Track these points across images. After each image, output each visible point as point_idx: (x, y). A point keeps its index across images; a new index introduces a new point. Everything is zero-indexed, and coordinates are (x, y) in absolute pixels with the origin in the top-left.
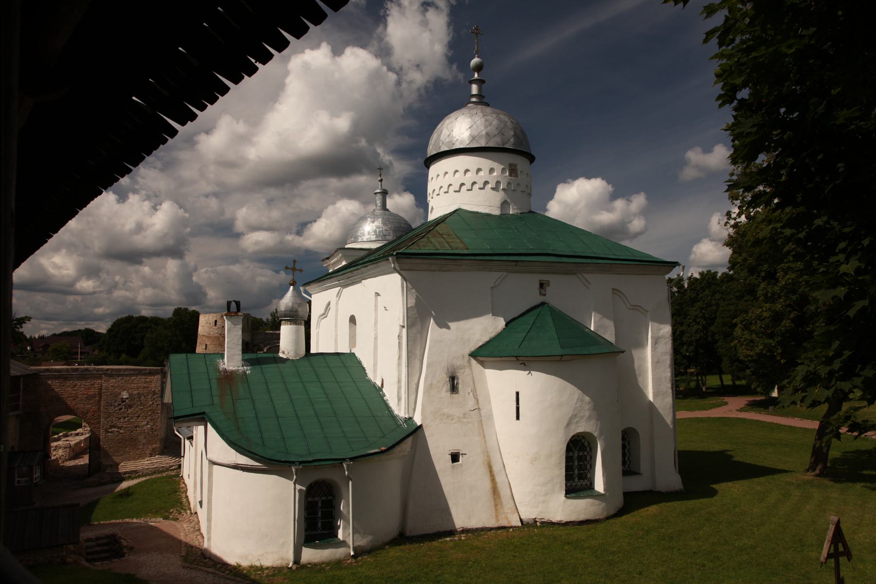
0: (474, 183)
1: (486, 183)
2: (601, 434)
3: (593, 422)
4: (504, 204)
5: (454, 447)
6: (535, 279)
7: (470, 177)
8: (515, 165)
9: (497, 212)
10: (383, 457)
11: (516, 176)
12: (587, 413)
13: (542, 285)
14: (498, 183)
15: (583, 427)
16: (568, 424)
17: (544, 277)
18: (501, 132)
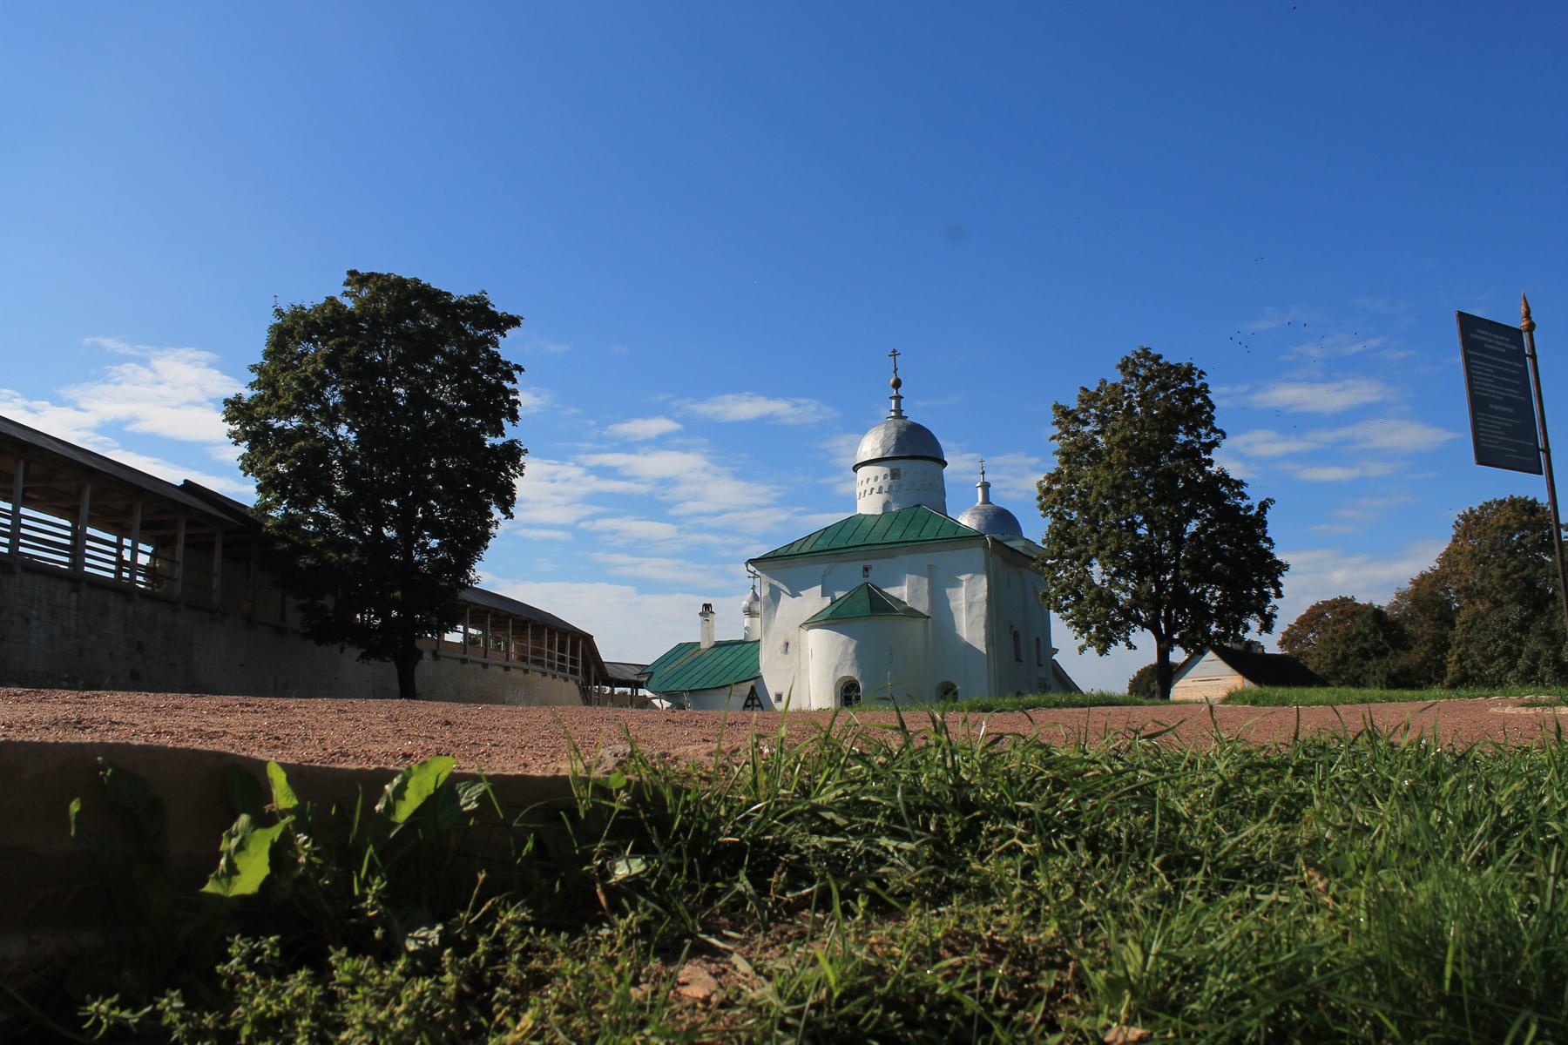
0: (873, 489)
1: (873, 489)
2: (861, 680)
3: (854, 669)
4: (886, 505)
5: (779, 691)
6: (860, 565)
7: (872, 484)
8: (899, 470)
9: (880, 512)
10: (716, 692)
11: (899, 478)
12: (849, 663)
13: (866, 569)
14: (881, 488)
15: (849, 672)
16: (836, 670)
17: (867, 563)
18: (883, 446)
